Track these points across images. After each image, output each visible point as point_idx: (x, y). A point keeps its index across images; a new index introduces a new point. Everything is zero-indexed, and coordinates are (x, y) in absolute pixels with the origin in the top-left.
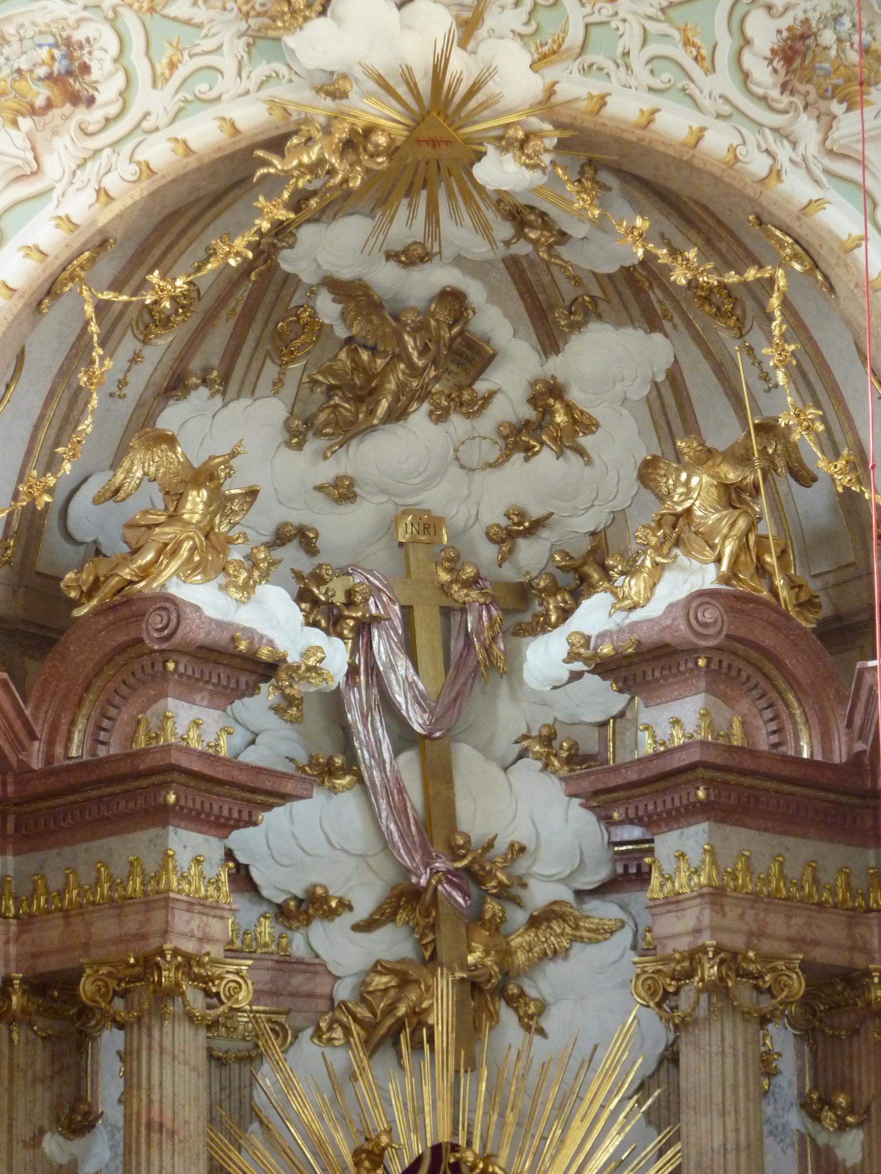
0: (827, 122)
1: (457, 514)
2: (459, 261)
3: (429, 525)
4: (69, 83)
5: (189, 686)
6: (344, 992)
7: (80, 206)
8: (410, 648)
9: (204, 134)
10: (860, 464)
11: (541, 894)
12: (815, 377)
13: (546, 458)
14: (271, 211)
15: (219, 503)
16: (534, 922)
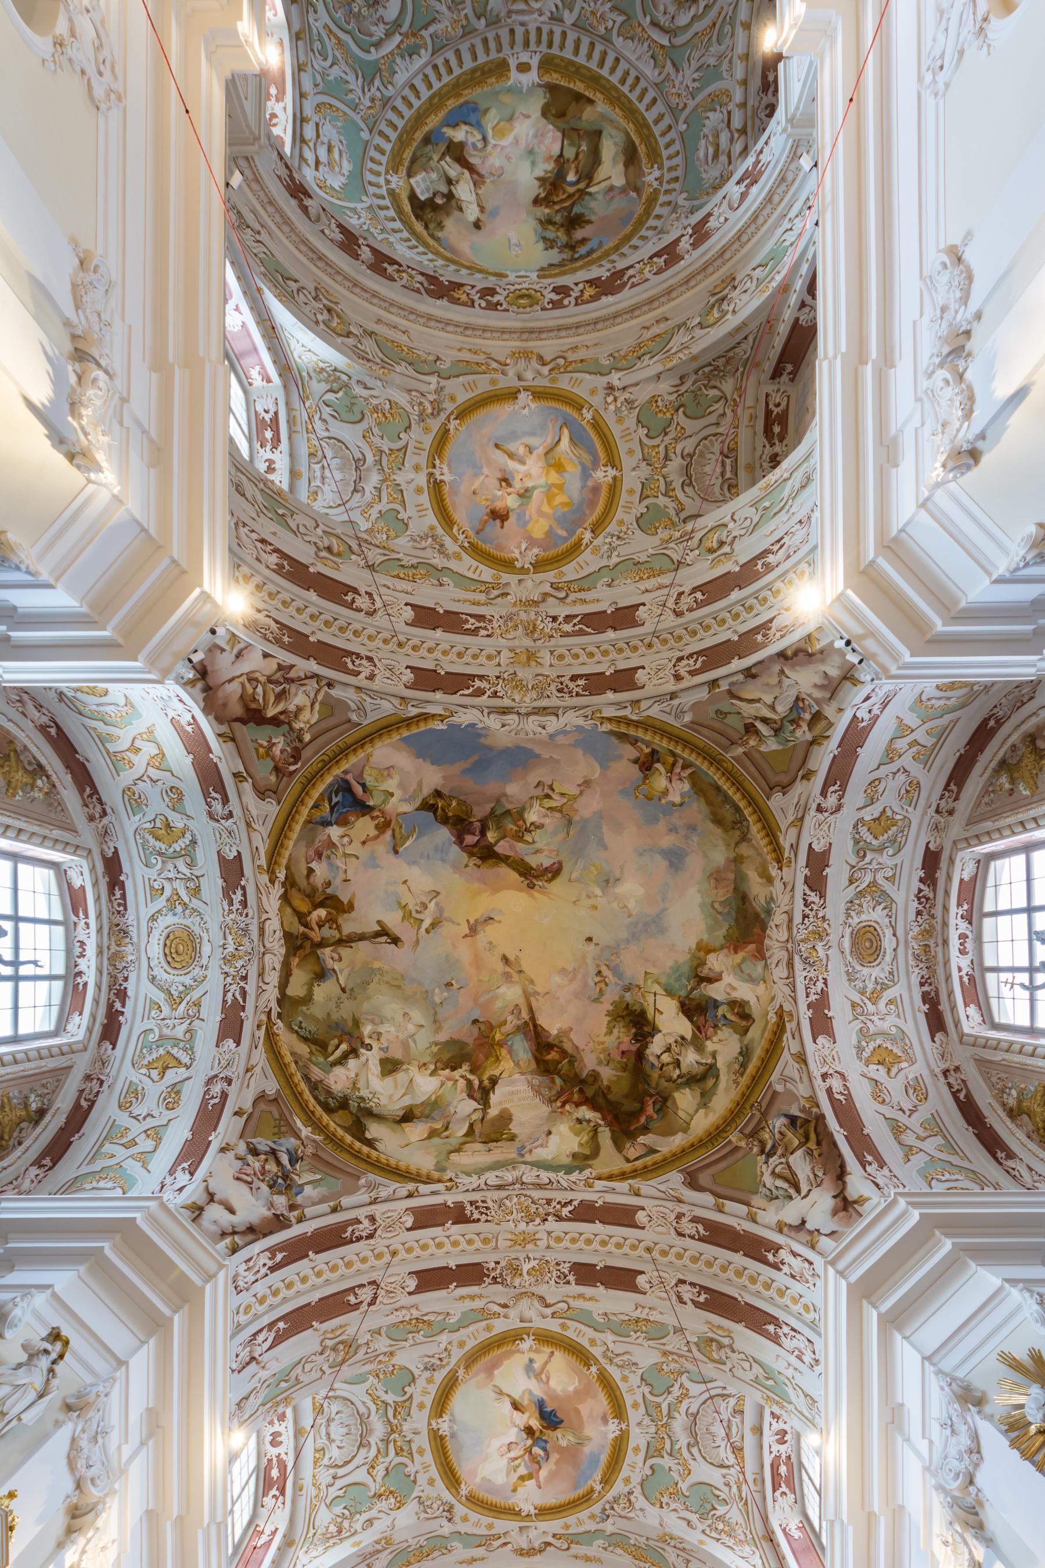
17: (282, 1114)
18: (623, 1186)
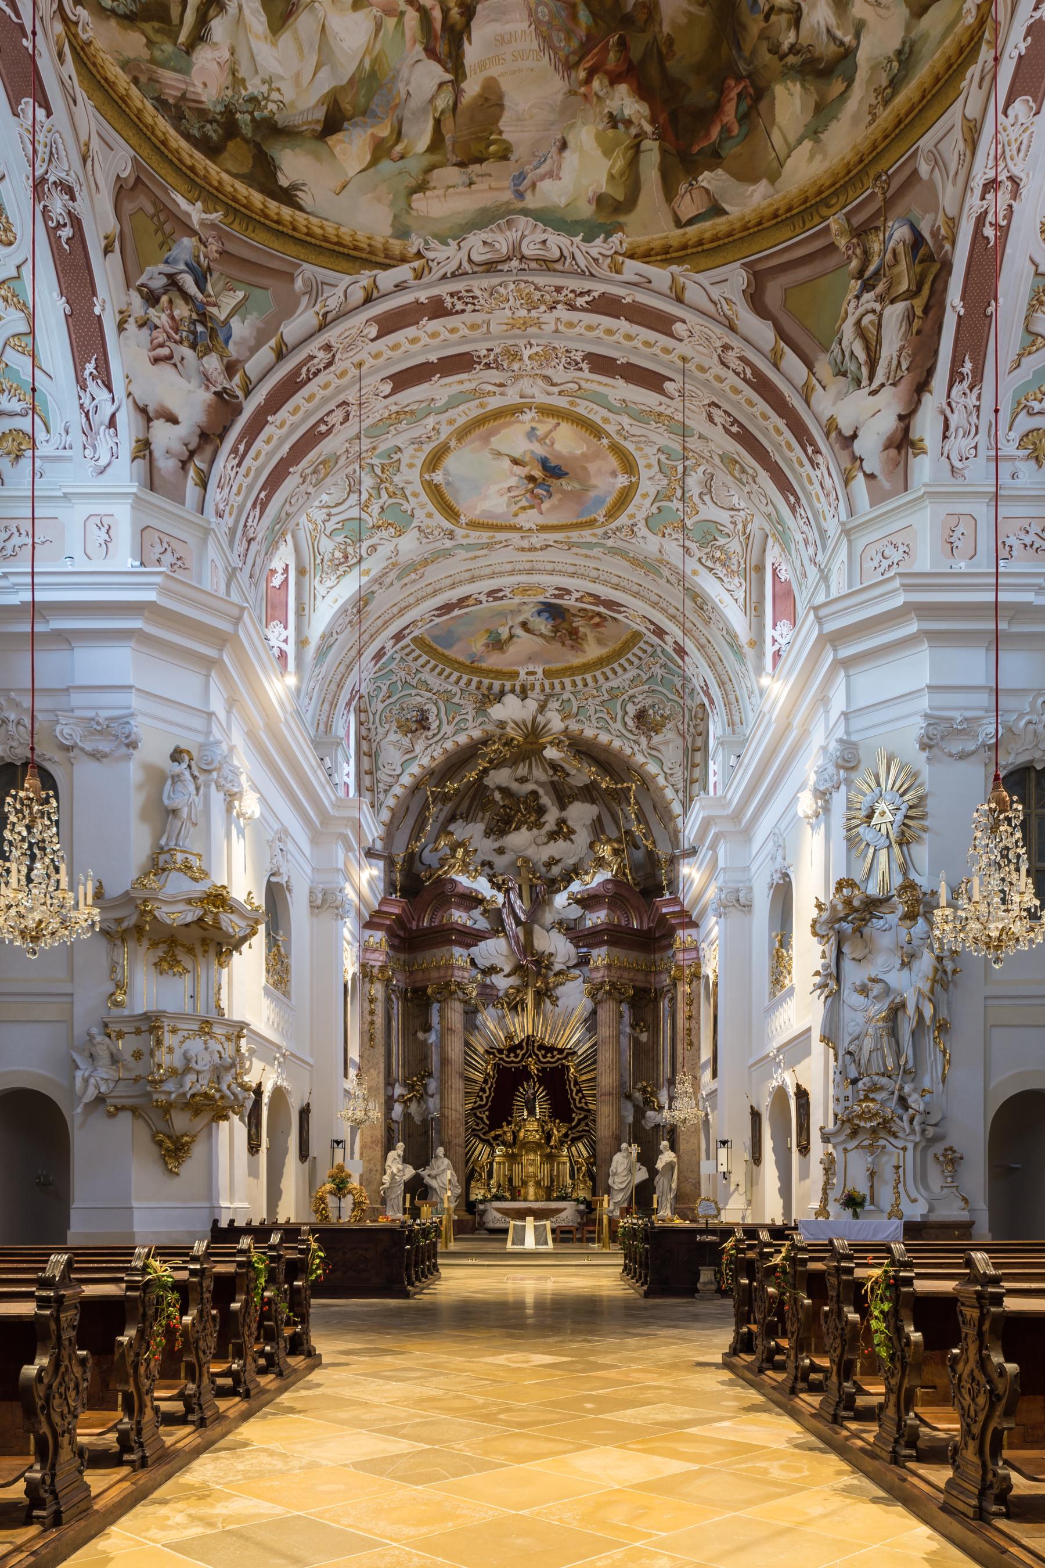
0: (649, 738)
1: (535, 858)
2: (537, 782)
3: (526, 860)
4: (423, 723)
5: (458, 906)
6: (501, 994)
7: (426, 761)
8: (521, 897)
9: (462, 739)
10: (654, 843)
11: (557, 967)
12: (641, 818)
13: (561, 842)
14: (483, 764)
15: (466, 853)
16: (555, 975)
17: (156, 201)
18: (661, 275)
